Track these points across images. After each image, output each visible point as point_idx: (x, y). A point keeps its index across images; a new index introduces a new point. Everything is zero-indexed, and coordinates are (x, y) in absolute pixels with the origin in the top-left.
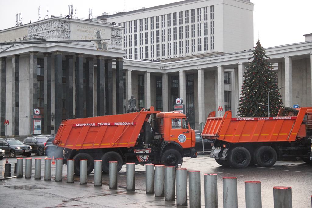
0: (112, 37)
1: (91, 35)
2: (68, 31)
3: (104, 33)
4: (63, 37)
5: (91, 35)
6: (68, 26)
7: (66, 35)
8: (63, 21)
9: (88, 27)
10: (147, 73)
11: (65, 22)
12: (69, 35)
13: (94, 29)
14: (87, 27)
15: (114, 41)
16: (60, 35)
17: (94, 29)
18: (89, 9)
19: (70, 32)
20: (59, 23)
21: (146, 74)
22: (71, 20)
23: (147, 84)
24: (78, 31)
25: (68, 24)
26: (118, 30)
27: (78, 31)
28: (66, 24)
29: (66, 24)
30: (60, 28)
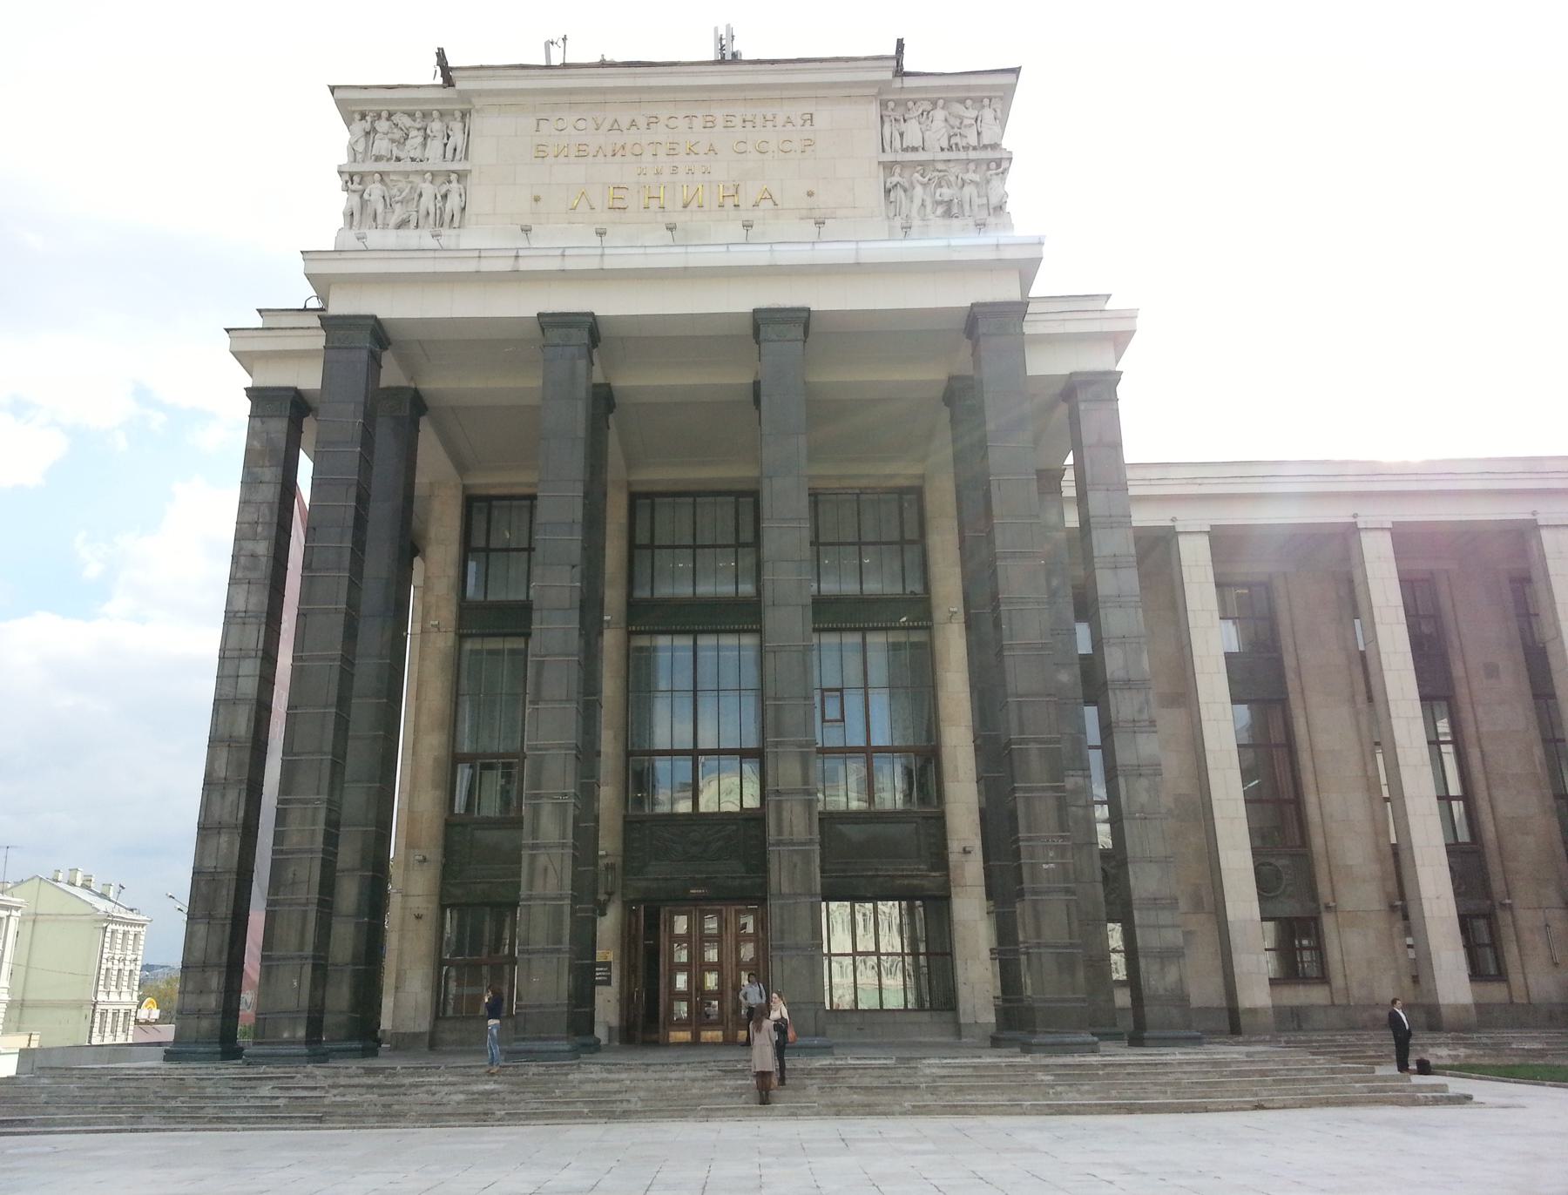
0: (888, 157)
1: (675, 170)
3: (809, 143)
4: (393, 220)
5: (675, 170)
6: (457, 138)
7: (427, 202)
8: (411, 115)
9: (642, 122)
10: (1544, 533)
12: (454, 202)
13: (698, 124)
14: (633, 124)
15: (919, 190)
16: (370, 210)
17: (698, 124)
18: (716, 30)
19: (462, 176)
20: (374, 130)
21: (1534, 542)
23: (1559, 607)
24: (540, 153)
25: (457, 126)
26: (962, 101)
27: (540, 153)
29: (436, 126)
30: (378, 158)
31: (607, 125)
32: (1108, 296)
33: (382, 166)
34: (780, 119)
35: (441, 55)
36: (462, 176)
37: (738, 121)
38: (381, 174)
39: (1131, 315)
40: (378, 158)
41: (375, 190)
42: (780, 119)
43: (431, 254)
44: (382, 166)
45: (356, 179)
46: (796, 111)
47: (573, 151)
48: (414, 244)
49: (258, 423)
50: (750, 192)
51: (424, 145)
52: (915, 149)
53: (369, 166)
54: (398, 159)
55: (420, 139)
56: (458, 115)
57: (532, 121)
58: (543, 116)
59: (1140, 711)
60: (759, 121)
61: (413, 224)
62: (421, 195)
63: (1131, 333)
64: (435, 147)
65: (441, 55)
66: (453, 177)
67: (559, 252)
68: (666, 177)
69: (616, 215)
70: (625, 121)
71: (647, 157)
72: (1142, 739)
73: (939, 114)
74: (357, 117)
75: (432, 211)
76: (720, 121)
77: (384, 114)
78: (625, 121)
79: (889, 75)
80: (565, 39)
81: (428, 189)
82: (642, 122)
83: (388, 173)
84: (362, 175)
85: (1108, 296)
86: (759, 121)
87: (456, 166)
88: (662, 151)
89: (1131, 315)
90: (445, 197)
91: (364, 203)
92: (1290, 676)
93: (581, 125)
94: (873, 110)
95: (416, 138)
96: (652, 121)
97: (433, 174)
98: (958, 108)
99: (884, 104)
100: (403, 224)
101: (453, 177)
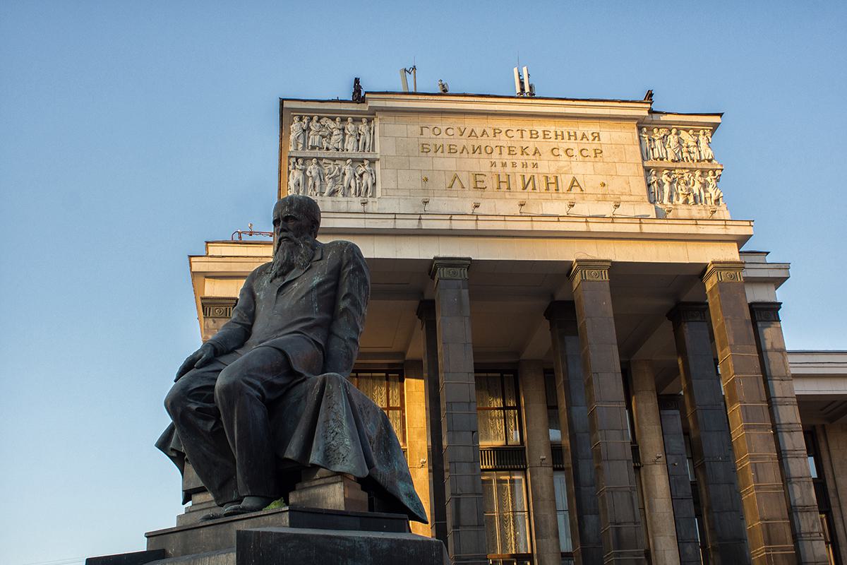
1: (514, 165)
2: (362, 161)
3: (598, 152)
4: (327, 191)
8: (334, 119)
11: (344, 120)
12: (367, 179)
13: (526, 134)
17: (526, 134)
19: (372, 162)
20: (309, 129)
22: (371, 103)
25: (363, 128)
26: (687, 130)
28: (350, 127)
29: (350, 127)
30: (313, 148)
31: (467, 133)
32: (768, 253)
33: (318, 153)
34: (579, 135)
35: (357, 81)
36: (372, 162)
37: (552, 135)
38: (318, 159)
39: (786, 267)
40: (313, 148)
41: (312, 169)
42: (579, 135)
43: (362, 216)
44: (318, 153)
45: (300, 161)
46: (589, 128)
47: (447, 148)
48: (343, 207)
49: (210, 322)
50: (565, 182)
51: (343, 141)
52: (662, 159)
53: (308, 153)
54: (328, 149)
55: (341, 136)
56: (364, 120)
57: (416, 128)
58: (424, 125)
59: (813, 526)
60: (566, 135)
61: (340, 194)
62: (344, 174)
63: (783, 280)
64: (350, 144)
65: (357, 81)
66: (366, 162)
67: (448, 217)
68: (509, 169)
69: (479, 193)
70: (479, 131)
71: (495, 155)
72: (816, 543)
73: (672, 139)
74: (296, 119)
75: (353, 185)
76: (541, 134)
77: (315, 118)
78: (479, 134)
79: (645, 113)
80: (414, 68)
81: (347, 169)
82: (490, 132)
83: (321, 159)
84: (305, 159)
85: (768, 253)
86: (566, 135)
87: (369, 156)
88: (505, 151)
89: (786, 267)
90: (361, 176)
91: (306, 178)
92: (832, 495)
93: (450, 132)
94: (636, 130)
95: (336, 137)
96: (496, 132)
97: (354, 160)
98: (683, 134)
99: (640, 129)
100: (333, 193)
101: (366, 162)
